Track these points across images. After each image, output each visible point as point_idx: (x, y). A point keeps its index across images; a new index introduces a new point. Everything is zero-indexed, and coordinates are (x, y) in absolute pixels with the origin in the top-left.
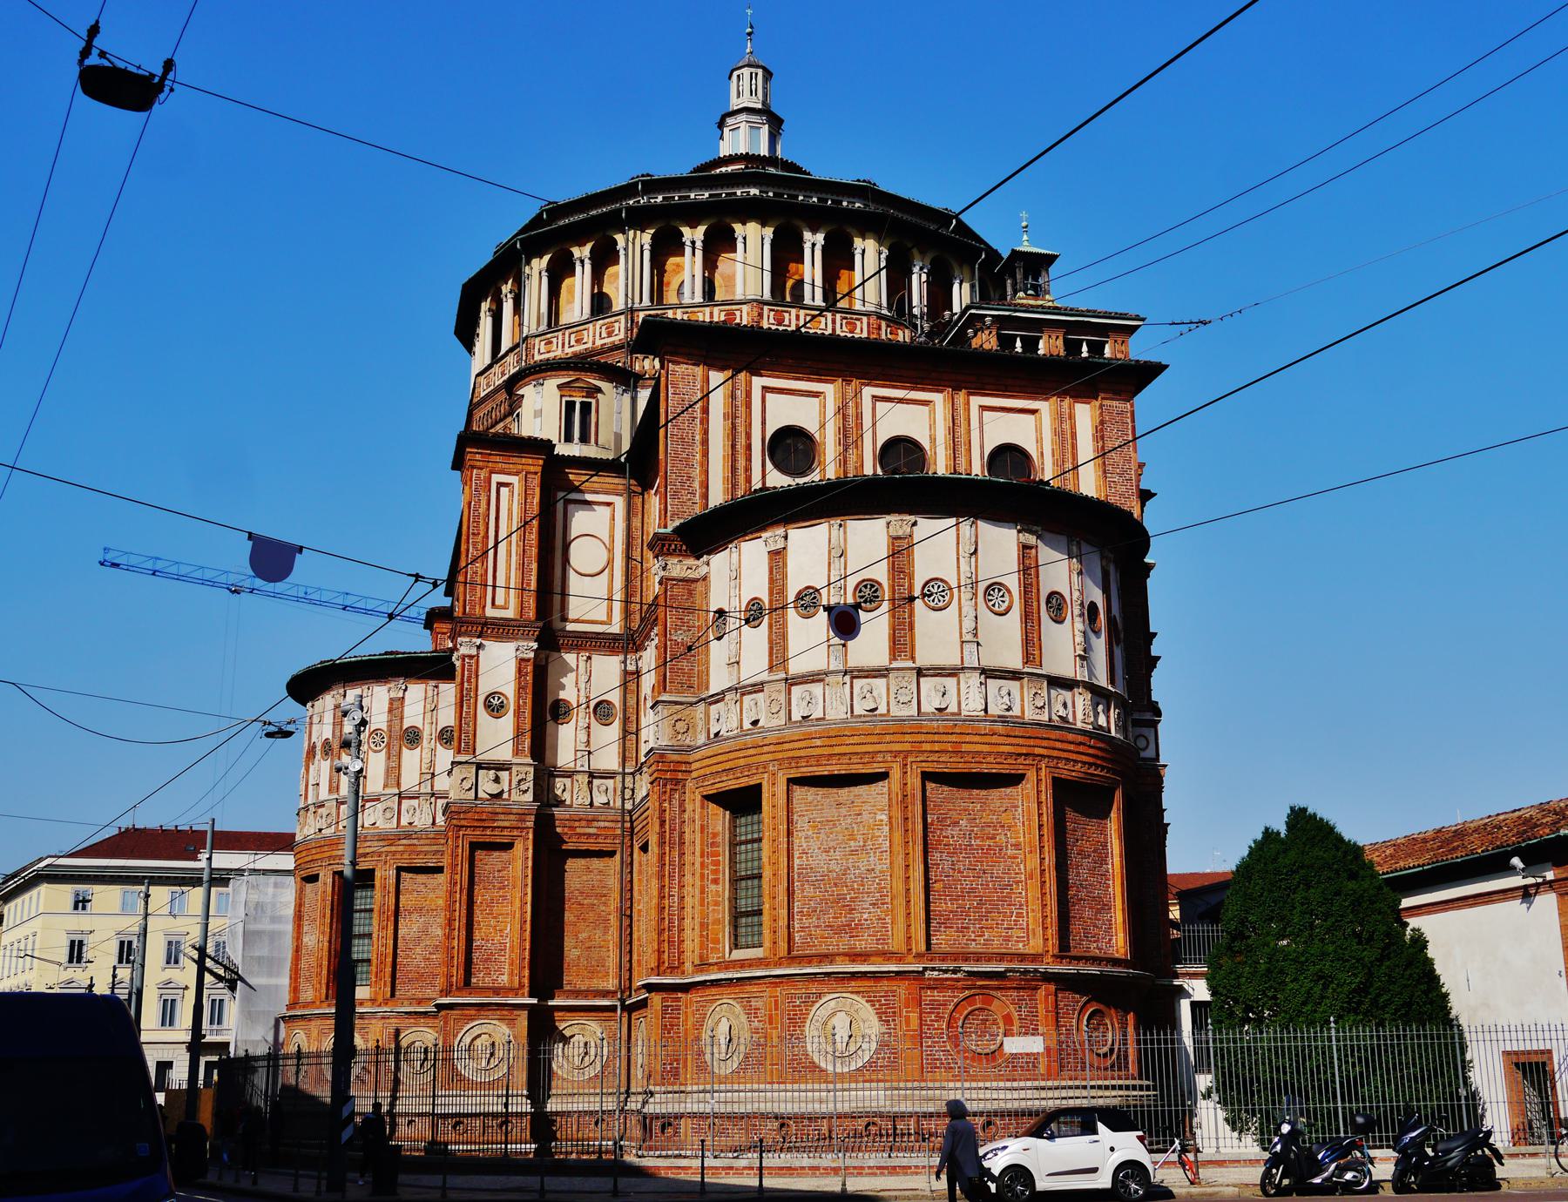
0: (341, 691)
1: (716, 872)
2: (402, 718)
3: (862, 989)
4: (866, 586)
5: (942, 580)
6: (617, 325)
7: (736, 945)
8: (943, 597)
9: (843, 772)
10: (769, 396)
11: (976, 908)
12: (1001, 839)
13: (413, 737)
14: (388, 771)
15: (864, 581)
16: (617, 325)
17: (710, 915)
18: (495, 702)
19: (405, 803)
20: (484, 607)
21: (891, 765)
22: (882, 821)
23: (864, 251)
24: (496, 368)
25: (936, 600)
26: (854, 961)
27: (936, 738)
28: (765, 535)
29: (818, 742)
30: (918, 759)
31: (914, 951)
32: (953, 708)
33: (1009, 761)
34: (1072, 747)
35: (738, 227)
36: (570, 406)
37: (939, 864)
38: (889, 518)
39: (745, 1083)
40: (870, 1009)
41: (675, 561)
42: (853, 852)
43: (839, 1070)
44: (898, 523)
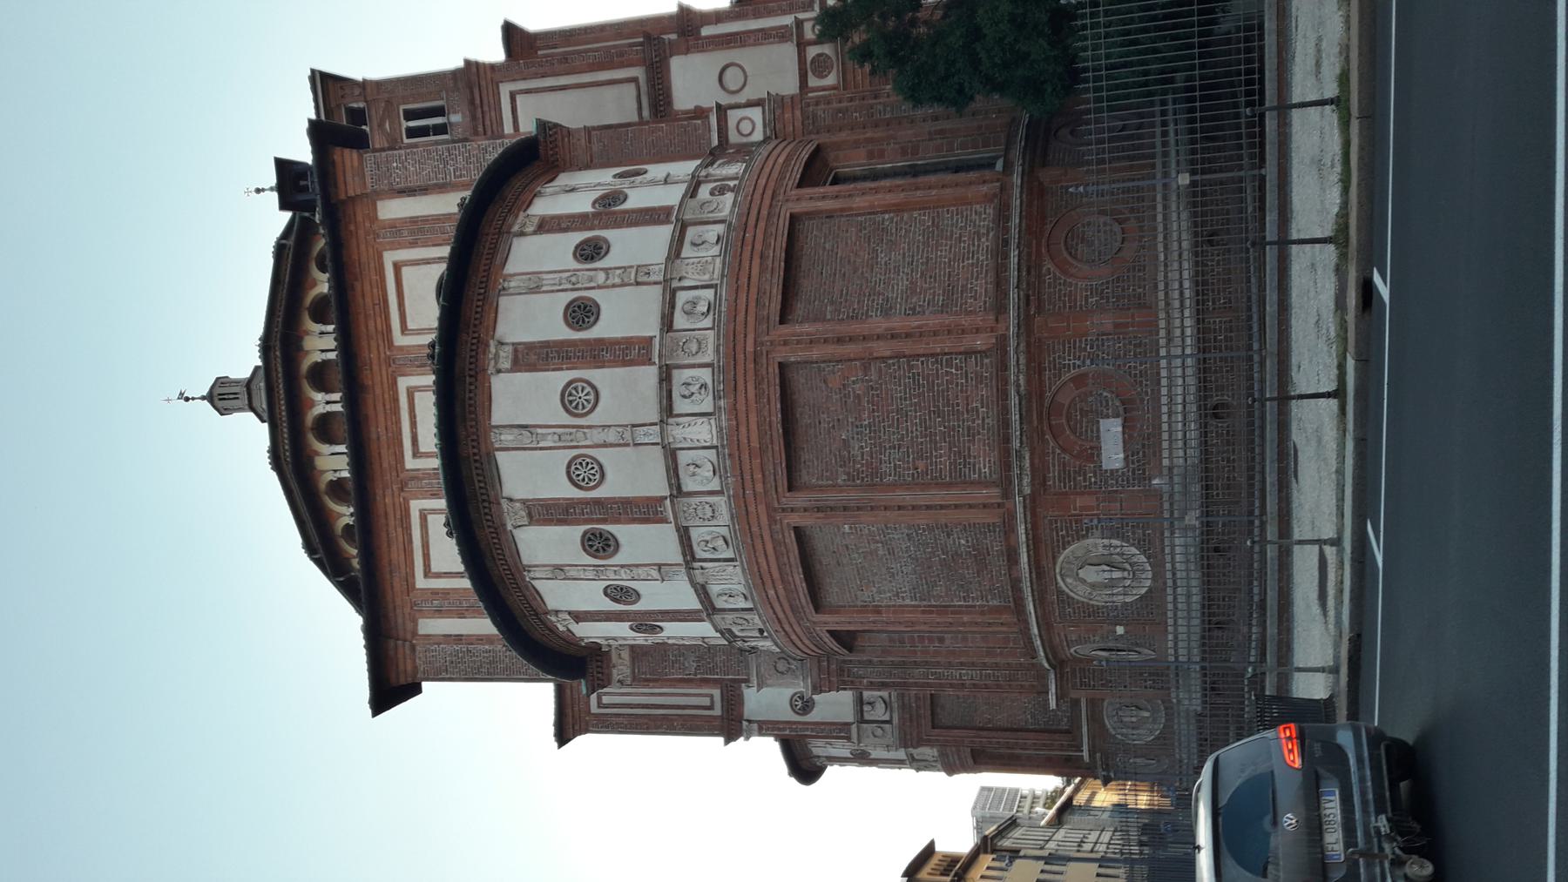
3: (1050, 554)
4: (591, 546)
5: (569, 466)
8: (588, 463)
9: (800, 570)
10: (434, 568)
11: (944, 418)
12: (859, 388)
15: (585, 550)
17: (978, 645)
21: (785, 525)
22: (851, 528)
23: (323, 351)
25: (592, 472)
27: (747, 477)
29: (771, 592)
31: (1000, 501)
33: (765, 386)
34: (743, 297)
35: (330, 476)
37: (895, 465)
38: (509, 527)
41: (615, 671)
42: (891, 552)
43: (1150, 575)
44: (512, 517)
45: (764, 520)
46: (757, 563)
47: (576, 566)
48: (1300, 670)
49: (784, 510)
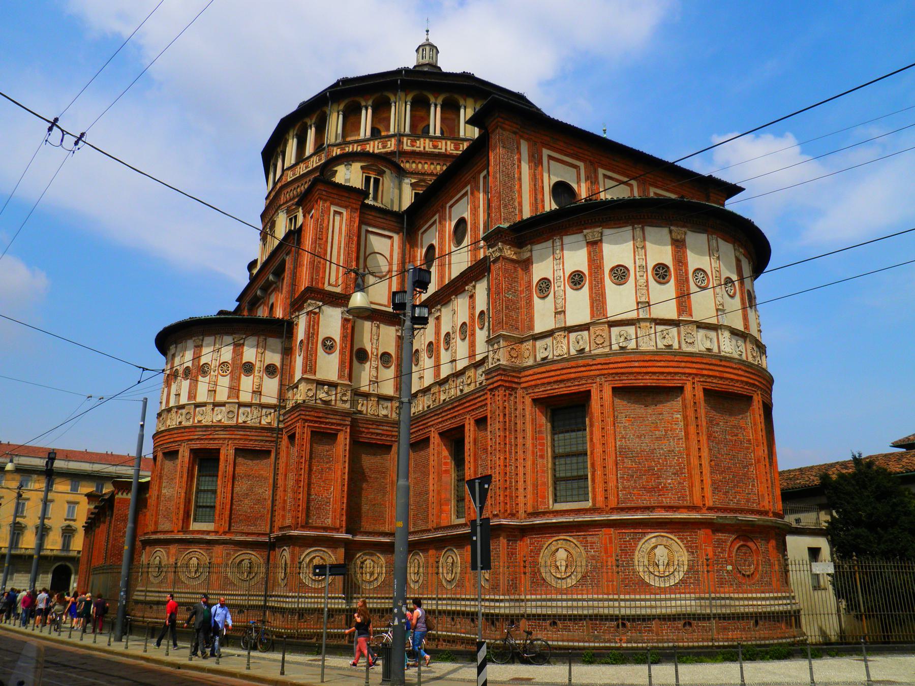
0: (201, 338)
1: (542, 450)
2: (242, 359)
6: (389, 143)
7: (555, 501)
13: (248, 368)
14: (231, 388)
16: (389, 143)
18: (328, 343)
19: (242, 410)
20: (324, 284)
22: (678, 418)
24: (302, 165)
26: (667, 511)
27: (711, 367)
28: (585, 231)
29: (636, 364)
30: (701, 380)
31: (707, 505)
32: (716, 350)
36: (368, 179)
39: (582, 594)
40: (681, 544)
43: (662, 585)
45: (688, 371)
46: (661, 361)
47: (646, 255)
48: (676, 667)
49: (694, 383)
